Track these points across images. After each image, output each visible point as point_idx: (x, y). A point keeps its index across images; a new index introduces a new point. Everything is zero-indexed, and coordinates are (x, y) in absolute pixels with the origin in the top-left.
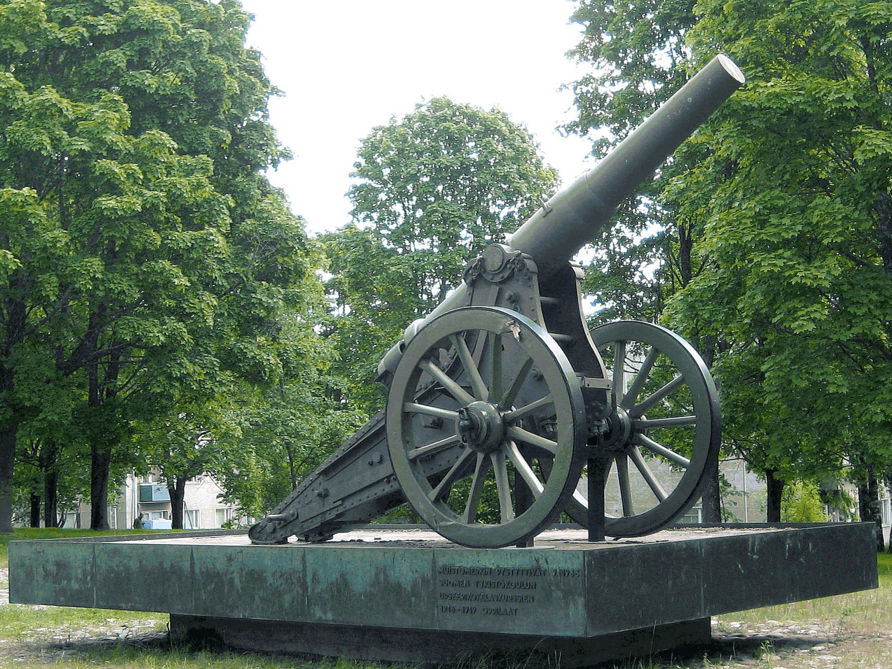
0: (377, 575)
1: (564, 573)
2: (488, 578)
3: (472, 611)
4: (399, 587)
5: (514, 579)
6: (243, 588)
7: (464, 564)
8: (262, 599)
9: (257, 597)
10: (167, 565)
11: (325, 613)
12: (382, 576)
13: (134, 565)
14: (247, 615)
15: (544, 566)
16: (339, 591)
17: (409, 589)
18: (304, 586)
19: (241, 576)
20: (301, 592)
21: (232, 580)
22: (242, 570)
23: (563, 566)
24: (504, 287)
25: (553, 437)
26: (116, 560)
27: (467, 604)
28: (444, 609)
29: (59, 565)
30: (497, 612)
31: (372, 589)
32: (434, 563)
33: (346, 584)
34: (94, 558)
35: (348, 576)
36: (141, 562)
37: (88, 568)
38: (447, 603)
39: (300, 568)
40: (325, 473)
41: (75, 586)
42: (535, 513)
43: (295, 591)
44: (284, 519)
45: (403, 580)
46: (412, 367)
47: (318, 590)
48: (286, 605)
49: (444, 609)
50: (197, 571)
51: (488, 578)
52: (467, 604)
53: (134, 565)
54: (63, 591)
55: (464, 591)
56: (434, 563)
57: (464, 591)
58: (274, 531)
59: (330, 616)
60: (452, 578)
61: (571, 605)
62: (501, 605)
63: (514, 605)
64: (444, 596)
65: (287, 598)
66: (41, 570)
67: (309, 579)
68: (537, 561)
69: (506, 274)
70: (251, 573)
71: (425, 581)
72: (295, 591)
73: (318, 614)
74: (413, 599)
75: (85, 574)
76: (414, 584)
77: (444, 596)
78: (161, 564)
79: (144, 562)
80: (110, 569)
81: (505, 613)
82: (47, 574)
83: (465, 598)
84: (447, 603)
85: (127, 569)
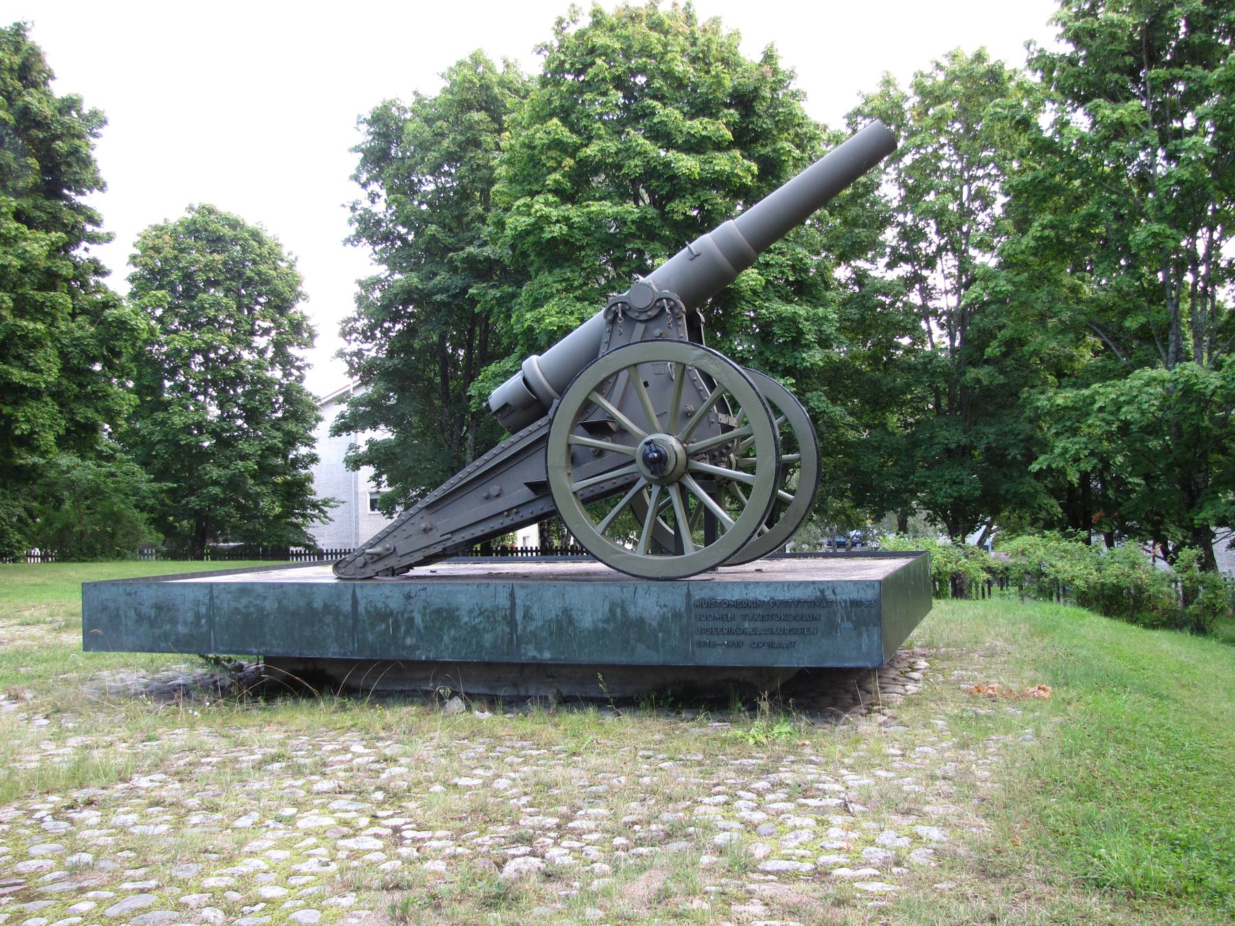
0: (612, 611)
1: (856, 603)
2: (759, 611)
3: (738, 645)
4: (641, 621)
5: (792, 611)
6: (426, 628)
7: (728, 597)
8: (454, 639)
9: (446, 638)
10: (318, 604)
11: (540, 651)
12: (619, 611)
13: (270, 605)
14: (432, 656)
15: (829, 595)
16: (560, 628)
17: (655, 624)
18: (512, 623)
19: (424, 615)
20: (508, 630)
21: (411, 620)
22: (425, 608)
23: (855, 596)
24: (651, 325)
25: (751, 469)
26: (244, 601)
27: (733, 638)
28: (700, 644)
29: (158, 607)
30: (771, 646)
31: (605, 626)
32: (689, 595)
33: (571, 621)
34: (212, 598)
35: (573, 613)
36: (280, 603)
37: (203, 610)
38: (705, 638)
39: (507, 604)
40: (429, 507)
41: (182, 629)
42: (723, 545)
43: (499, 629)
44: (378, 554)
45: (646, 615)
46: (582, 398)
47: (531, 628)
48: (487, 645)
49: (700, 644)
50: (361, 609)
51: (759, 611)
52: (733, 638)
53: (270, 605)
54: (166, 636)
55: (727, 625)
56: (689, 595)
57: (727, 625)
58: (365, 564)
59: (547, 655)
60: (715, 612)
61: (865, 635)
62: (776, 639)
63: (794, 638)
64: (704, 631)
65: (488, 638)
66: (132, 613)
67: (519, 616)
68: (822, 592)
69: (652, 313)
70: (438, 611)
71: (677, 615)
72: (499, 629)
73: (530, 653)
74: (660, 635)
75: (198, 616)
76: (663, 618)
77: (704, 631)
78: (309, 604)
79: (285, 602)
80: (237, 611)
81: (780, 646)
82: (140, 618)
83: (730, 632)
84: (705, 638)
85: (261, 610)
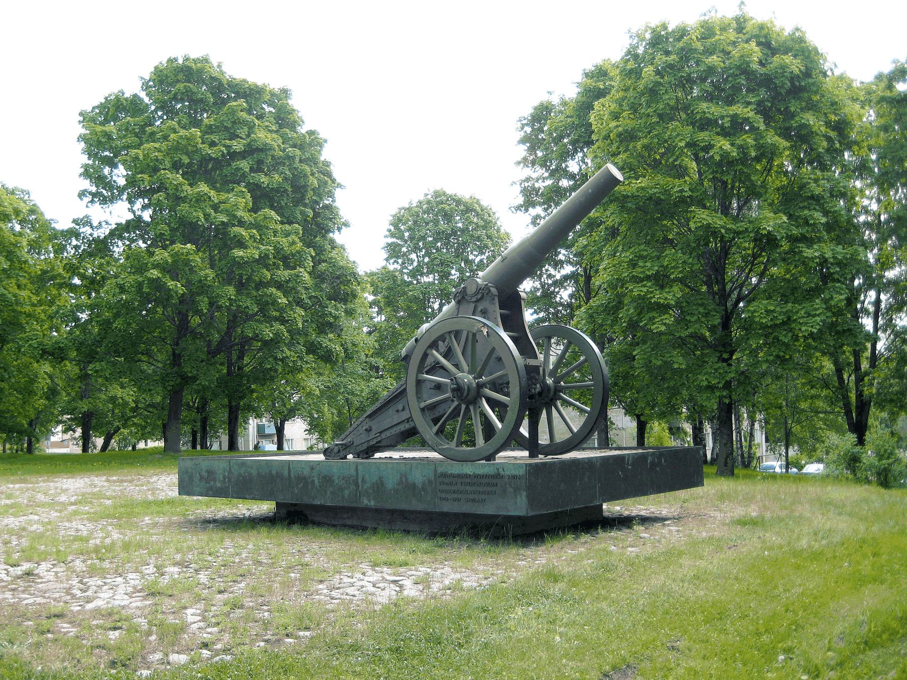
1: (514, 477)
2: (468, 480)
3: (459, 500)
4: (414, 485)
5: (484, 481)
7: (454, 472)
8: (332, 493)
10: (274, 472)
13: (254, 472)
16: (378, 488)
18: (357, 484)
21: (313, 481)
23: (514, 472)
24: (479, 304)
25: (507, 395)
27: (455, 496)
29: (208, 472)
30: (474, 500)
32: (436, 471)
38: (443, 495)
39: (355, 474)
40: (370, 416)
41: (219, 485)
42: (496, 441)
44: (345, 445)
45: (416, 481)
47: (365, 487)
48: (346, 496)
51: (468, 480)
52: (455, 496)
53: (254, 472)
54: (211, 488)
56: (436, 471)
58: (339, 451)
59: (372, 503)
60: (447, 480)
63: (484, 497)
64: (442, 491)
65: (347, 492)
66: (198, 475)
67: (360, 481)
69: (479, 296)
70: (325, 477)
71: (430, 481)
75: (224, 478)
76: (424, 484)
77: (442, 491)
78: (270, 471)
81: (479, 501)
82: (201, 478)
83: (454, 492)
84: (443, 495)
85: (250, 474)
